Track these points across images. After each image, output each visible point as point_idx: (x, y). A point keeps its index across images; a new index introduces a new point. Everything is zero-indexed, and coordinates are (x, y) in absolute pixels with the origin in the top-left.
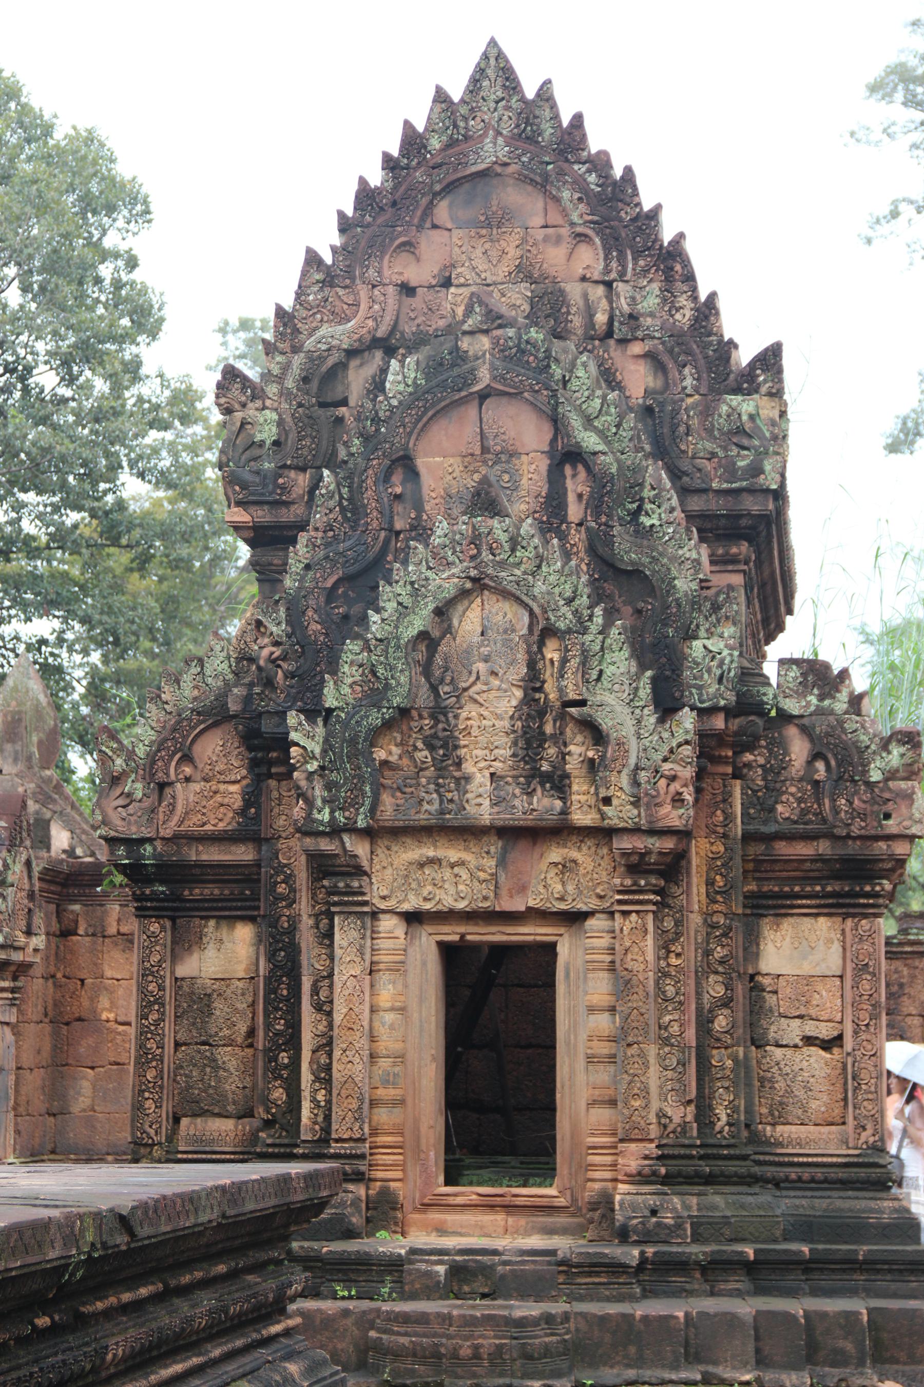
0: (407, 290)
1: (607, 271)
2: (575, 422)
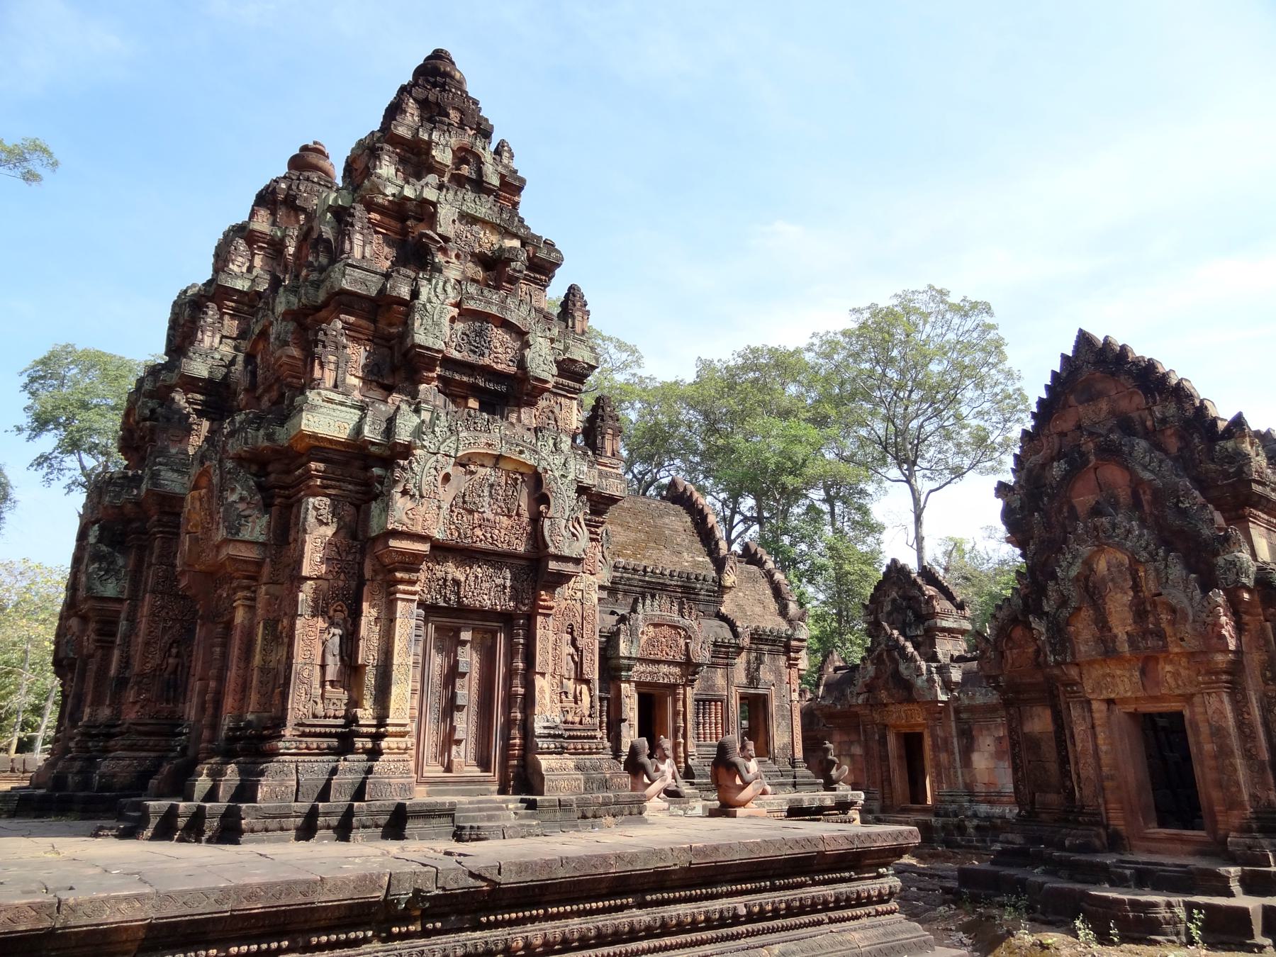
0: (1062, 434)
1: (1147, 403)
2: (1139, 469)
